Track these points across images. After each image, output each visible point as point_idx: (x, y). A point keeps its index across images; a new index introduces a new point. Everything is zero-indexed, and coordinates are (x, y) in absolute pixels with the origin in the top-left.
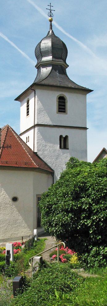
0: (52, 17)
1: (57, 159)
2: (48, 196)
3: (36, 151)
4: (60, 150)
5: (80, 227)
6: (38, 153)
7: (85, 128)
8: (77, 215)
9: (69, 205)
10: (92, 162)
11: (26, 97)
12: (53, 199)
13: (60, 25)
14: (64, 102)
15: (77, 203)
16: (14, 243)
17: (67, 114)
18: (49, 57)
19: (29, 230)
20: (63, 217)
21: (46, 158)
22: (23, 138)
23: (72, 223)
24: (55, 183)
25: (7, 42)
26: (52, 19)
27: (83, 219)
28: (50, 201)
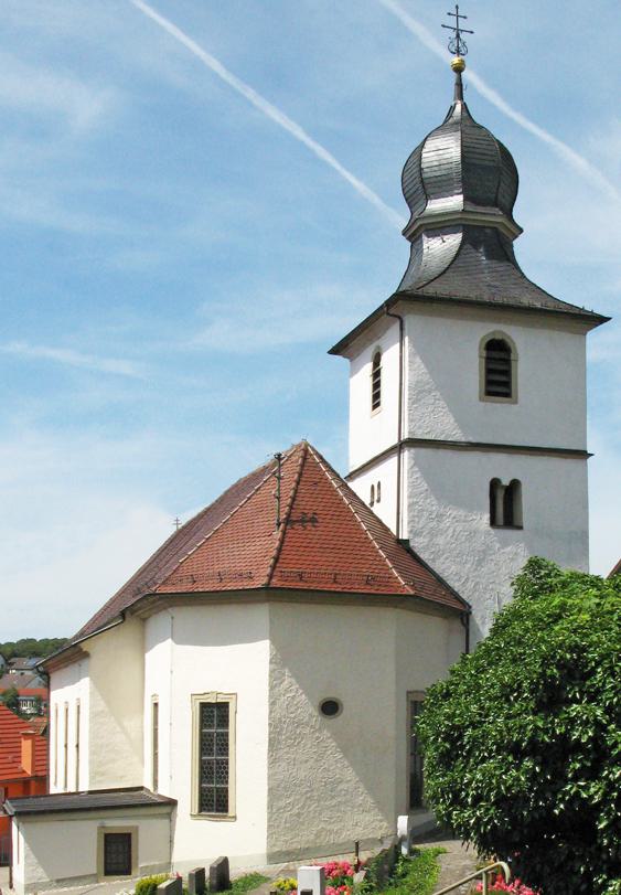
0: (461, 57)
1: (480, 563)
2: (447, 695)
3: (404, 535)
4: (493, 531)
5: (562, 806)
6: (411, 544)
7: (583, 455)
8: (554, 763)
9: (523, 727)
10: (605, 575)
11: (371, 341)
12: (467, 708)
13: (493, 86)
14: (507, 362)
15: (552, 722)
16: (329, 864)
17: (516, 402)
18: (450, 198)
19: (379, 818)
20: (503, 773)
21: (442, 560)
22: (361, 487)
23: (536, 792)
24: (472, 651)
25: (302, 144)
26: (462, 62)
27: (576, 779)
28: (454, 714)
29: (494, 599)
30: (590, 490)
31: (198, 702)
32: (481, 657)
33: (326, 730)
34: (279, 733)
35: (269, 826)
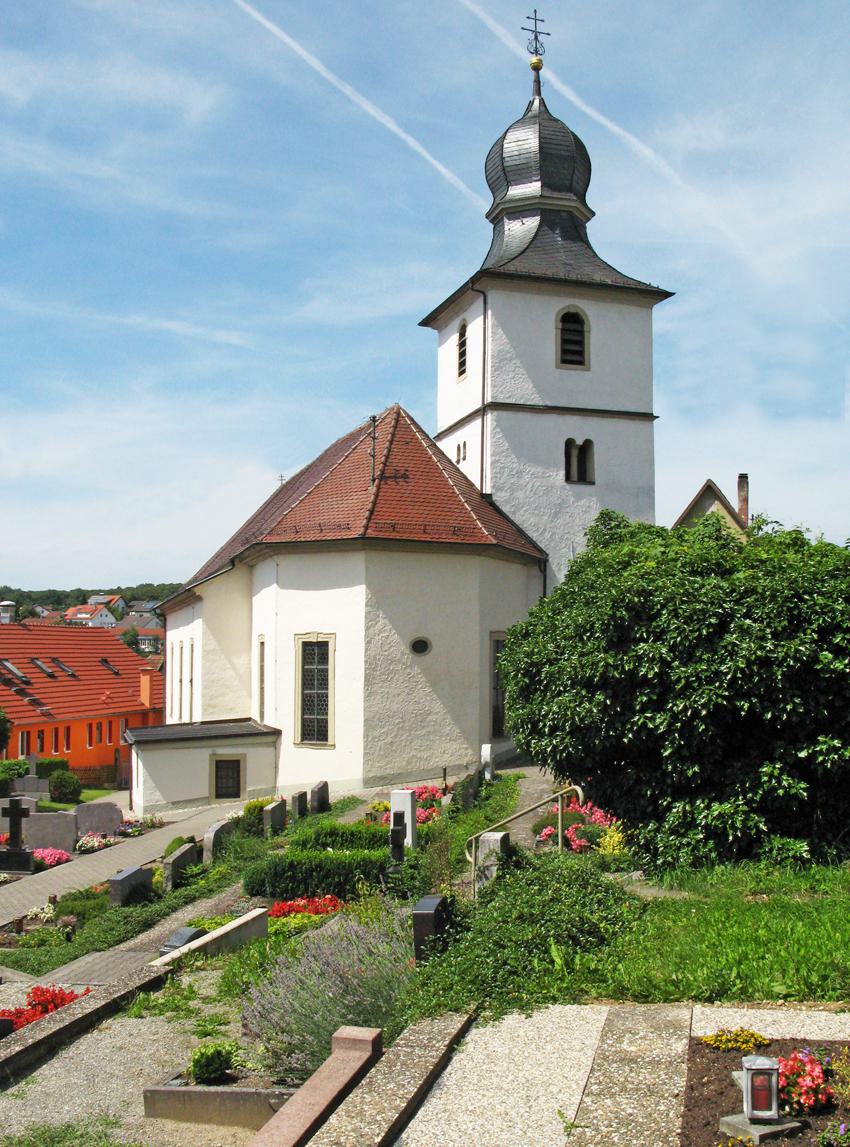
0: (539, 57)
1: (556, 515)
2: (526, 635)
3: (487, 490)
4: (568, 487)
5: (630, 735)
6: (494, 498)
7: (649, 417)
8: (623, 697)
9: (595, 664)
10: (669, 526)
11: (457, 314)
12: (544, 647)
13: (568, 82)
14: (581, 333)
15: (622, 659)
16: (419, 788)
17: (588, 370)
18: (529, 184)
19: (465, 746)
20: (577, 706)
21: (522, 512)
22: (448, 446)
23: (607, 723)
24: (549, 595)
25: (394, 136)
26: (540, 61)
27: (643, 711)
28: (532, 652)
29: (569, 548)
30: (655, 449)
31: (300, 641)
32: (557, 601)
33: (416, 667)
34: (374, 670)
35: (365, 754)
